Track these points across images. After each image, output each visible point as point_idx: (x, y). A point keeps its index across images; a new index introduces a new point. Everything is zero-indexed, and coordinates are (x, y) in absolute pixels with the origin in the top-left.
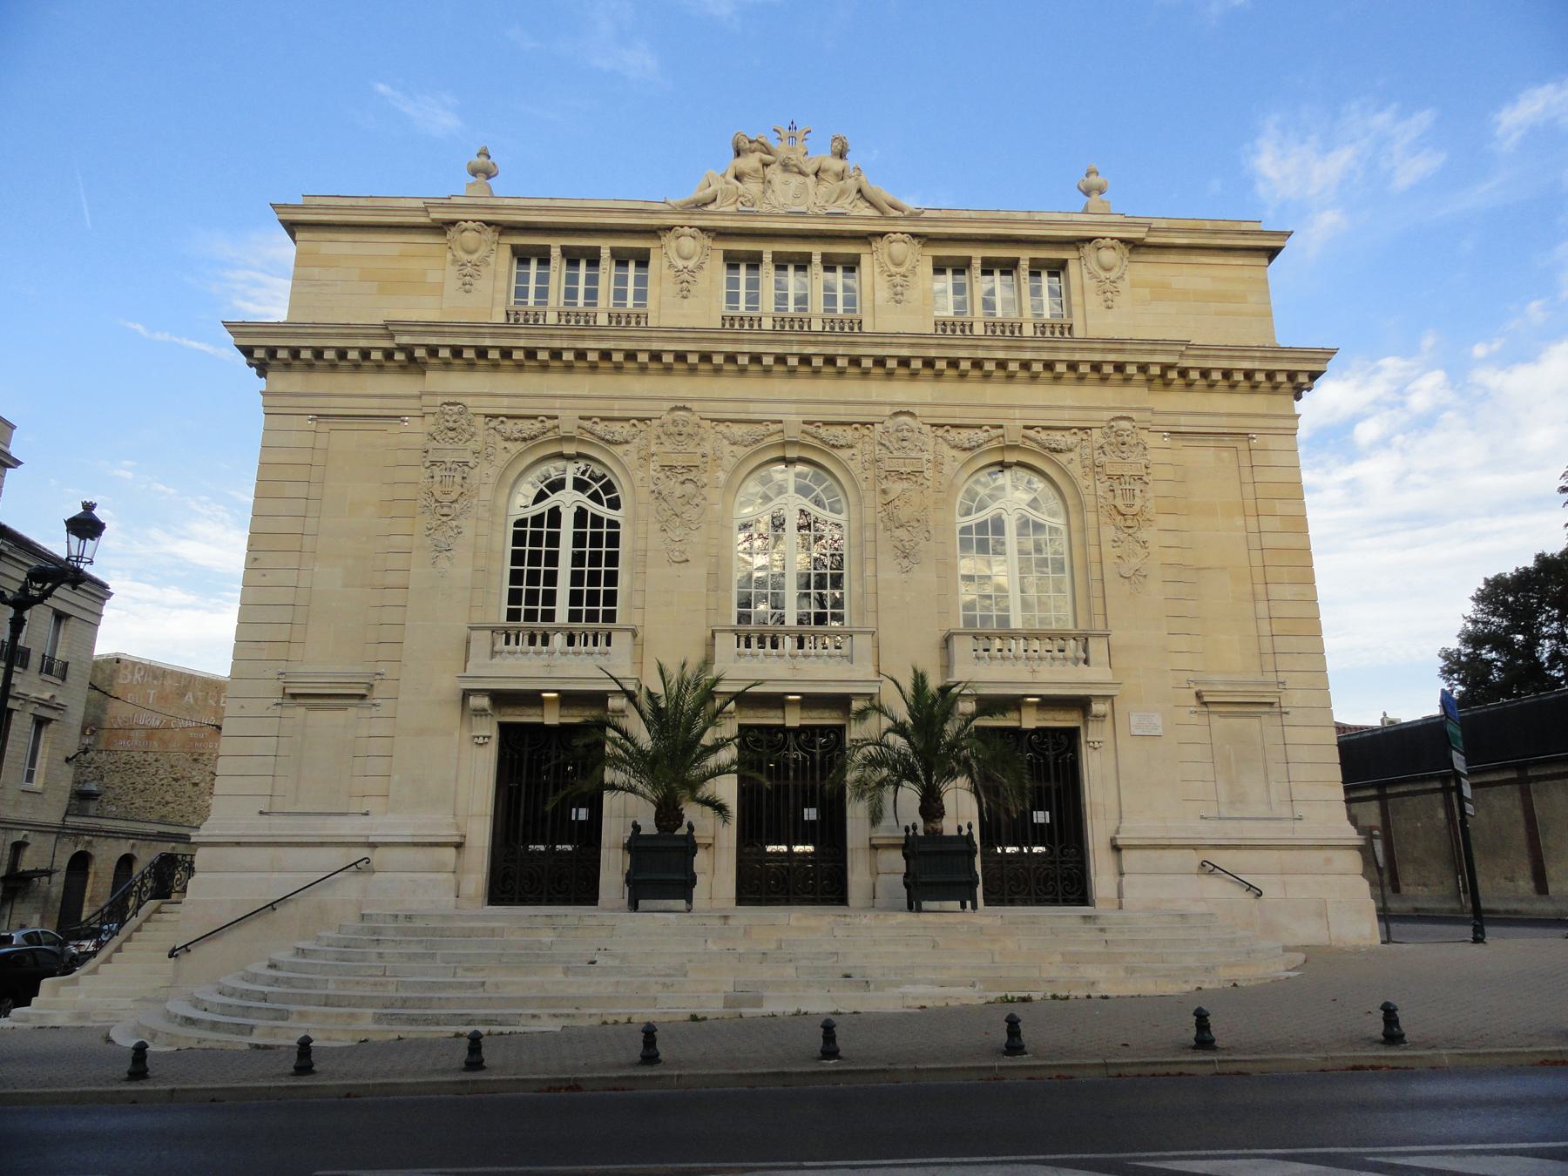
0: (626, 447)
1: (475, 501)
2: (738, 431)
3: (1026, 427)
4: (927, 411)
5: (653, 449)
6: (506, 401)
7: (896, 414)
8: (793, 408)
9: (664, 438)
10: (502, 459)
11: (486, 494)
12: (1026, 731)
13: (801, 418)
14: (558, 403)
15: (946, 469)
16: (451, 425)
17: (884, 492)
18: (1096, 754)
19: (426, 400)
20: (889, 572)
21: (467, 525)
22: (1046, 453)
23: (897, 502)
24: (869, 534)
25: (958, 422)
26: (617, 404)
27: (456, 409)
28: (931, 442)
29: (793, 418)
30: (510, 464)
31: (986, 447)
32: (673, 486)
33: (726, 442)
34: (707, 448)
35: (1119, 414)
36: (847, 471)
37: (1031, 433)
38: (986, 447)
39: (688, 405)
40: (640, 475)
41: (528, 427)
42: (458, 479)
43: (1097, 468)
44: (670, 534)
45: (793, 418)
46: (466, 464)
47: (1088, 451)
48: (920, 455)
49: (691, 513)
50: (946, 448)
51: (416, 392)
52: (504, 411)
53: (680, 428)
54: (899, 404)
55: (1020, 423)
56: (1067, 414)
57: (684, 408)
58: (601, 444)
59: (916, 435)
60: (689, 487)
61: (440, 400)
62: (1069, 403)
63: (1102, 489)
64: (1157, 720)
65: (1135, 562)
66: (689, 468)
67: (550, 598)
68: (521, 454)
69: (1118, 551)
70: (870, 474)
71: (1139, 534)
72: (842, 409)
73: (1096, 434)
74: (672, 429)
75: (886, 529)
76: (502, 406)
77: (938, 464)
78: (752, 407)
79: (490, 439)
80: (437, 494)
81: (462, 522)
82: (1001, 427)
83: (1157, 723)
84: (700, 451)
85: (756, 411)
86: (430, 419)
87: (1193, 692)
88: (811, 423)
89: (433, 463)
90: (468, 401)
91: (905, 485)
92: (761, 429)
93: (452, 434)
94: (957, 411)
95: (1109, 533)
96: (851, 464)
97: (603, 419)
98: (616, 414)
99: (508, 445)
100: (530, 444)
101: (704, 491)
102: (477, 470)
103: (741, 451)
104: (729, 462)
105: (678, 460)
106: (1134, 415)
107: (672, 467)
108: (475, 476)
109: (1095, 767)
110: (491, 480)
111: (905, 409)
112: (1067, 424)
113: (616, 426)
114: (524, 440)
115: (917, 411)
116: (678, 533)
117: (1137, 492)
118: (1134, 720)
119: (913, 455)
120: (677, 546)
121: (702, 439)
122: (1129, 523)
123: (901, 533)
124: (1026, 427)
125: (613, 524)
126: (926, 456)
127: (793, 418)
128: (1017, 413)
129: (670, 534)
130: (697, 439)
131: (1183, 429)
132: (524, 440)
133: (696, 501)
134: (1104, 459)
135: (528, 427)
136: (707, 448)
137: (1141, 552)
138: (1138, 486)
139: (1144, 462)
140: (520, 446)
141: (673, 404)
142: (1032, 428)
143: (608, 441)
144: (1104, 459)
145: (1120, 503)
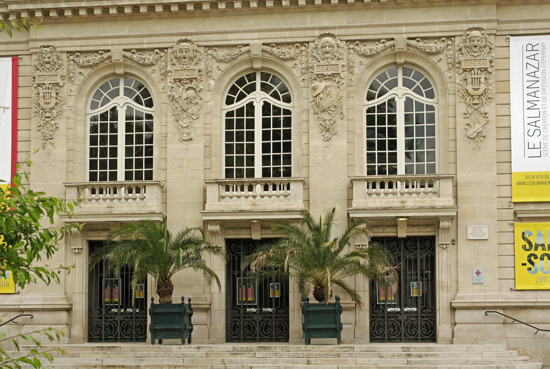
0: (154, 68)
1: (65, 107)
2: (221, 53)
3: (409, 39)
4: (343, 32)
5: (169, 68)
6: (78, 42)
7: (325, 35)
8: (256, 35)
9: (175, 61)
10: (79, 79)
11: (71, 102)
12: (400, 239)
13: (261, 42)
14: (110, 41)
15: (356, 71)
16: (47, 60)
17: (314, 89)
18: (445, 252)
19: (31, 44)
20: (317, 141)
21: (62, 123)
22: (423, 55)
23: (321, 95)
24: (304, 117)
25: (364, 38)
26: (146, 40)
27: (48, 50)
28: (345, 52)
29: (256, 42)
30: (84, 82)
31: (383, 54)
32: (182, 93)
33: (214, 60)
34: (202, 66)
35: (472, 26)
36: (292, 75)
37: (413, 42)
38: (383, 54)
39: (189, 38)
40: (162, 85)
41: (93, 59)
42: (54, 94)
43: (455, 65)
44: (181, 123)
45: (256, 42)
46: (57, 84)
47: (451, 52)
48: (337, 62)
49: (193, 109)
50: (356, 56)
51: (25, 39)
52: (78, 49)
53: (184, 54)
54: (325, 28)
55: (405, 36)
56: (438, 28)
57: (186, 41)
58: (138, 66)
59: (336, 48)
60: (191, 92)
61: (39, 44)
62: (440, 19)
63: (459, 79)
64: (485, 230)
65: (478, 127)
66: (191, 80)
67: (114, 165)
68: (90, 75)
69: (467, 121)
70: (305, 77)
71: (482, 109)
72: (287, 34)
73: (458, 40)
74: (179, 55)
75: (315, 113)
76: (76, 46)
77: (350, 68)
78: (230, 36)
79: (71, 67)
80: (42, 104)
81: (58, 121)
82: (393, 39)
83: (484, 232)
84: (197, 68)
85: (233, 39)
86: (34, 57)
87: (512, 211)
88: (268, 44)
89: (39, 85)
90: (56, 44)
91: (328, 83)
92: (236, 51)
93: (48, 66)
94: (364, 31)
95: (462, 108)
96: (294, 71)
97: (138, 50)
98: (145, 46)
99: (82, 71)
100: (96, 69)
101: (201, 94)
102: (65, 88)
103: (223, 66)
104: (216, 74)
105: (184, 75)
106: (484, 26)
107: (180, 80)
108: (64, 92)
109: (442, 258)
110: (74, 93)
111: (327, 32)
112: (438, 34)
113: (146, 55)
114: (91, 66)
115: (336, 32)
116: (185, 122)
117: (482, 80)
118: (470, 230)
119: (334, 62)
120: (185, 131)
121: (200, 60)
122: (476, 101)
123: (325, 116)
124: (409, 39)
125: (149, 117)
126: (341, 63)
127: (256, 42)
128: (404, 29)
129: (181, 123)
130: (195, 60)
131: (520, 32)
132: (91, 66)
133: (196, 101)
134: (462, 58)
135: (93, 59)
136: (202, 66)
137: (483, 121)
138: (483, 76)
139: (488, 58)
140: (89, 71)
141: (179, 38)
142: (414, 39)
143: (141, 64)
144: (462, 58)
145: (470, 88)
